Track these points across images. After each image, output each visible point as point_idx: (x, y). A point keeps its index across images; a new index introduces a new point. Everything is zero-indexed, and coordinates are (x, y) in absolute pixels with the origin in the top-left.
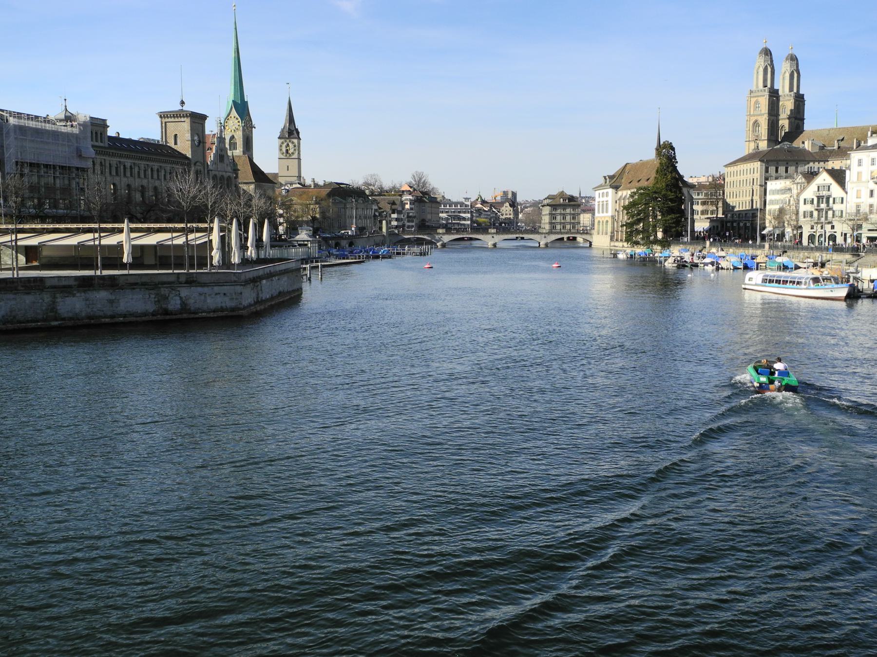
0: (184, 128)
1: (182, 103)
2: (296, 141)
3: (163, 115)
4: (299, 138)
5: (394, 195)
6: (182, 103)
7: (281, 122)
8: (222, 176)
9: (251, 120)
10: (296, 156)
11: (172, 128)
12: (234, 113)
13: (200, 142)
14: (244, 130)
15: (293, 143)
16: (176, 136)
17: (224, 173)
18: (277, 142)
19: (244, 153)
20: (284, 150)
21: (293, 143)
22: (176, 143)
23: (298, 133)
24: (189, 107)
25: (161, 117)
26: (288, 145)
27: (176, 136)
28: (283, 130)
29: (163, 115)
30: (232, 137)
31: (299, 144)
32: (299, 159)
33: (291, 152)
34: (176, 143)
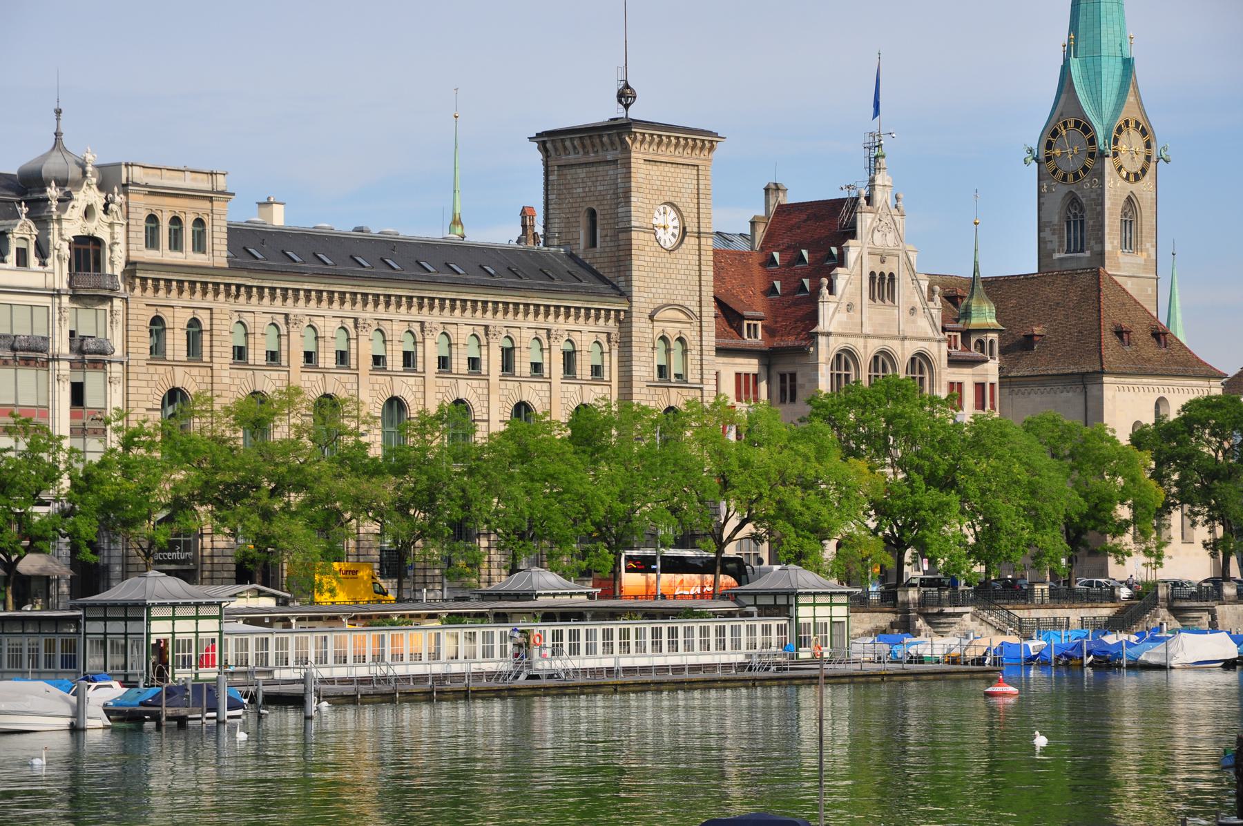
1: (625, 96)
3: (549, 141)
6: (625, 96)
16: (592, 213)
17: (894, 346)
24: (635, 113)
25: (543, 148)
29: (549, 141)
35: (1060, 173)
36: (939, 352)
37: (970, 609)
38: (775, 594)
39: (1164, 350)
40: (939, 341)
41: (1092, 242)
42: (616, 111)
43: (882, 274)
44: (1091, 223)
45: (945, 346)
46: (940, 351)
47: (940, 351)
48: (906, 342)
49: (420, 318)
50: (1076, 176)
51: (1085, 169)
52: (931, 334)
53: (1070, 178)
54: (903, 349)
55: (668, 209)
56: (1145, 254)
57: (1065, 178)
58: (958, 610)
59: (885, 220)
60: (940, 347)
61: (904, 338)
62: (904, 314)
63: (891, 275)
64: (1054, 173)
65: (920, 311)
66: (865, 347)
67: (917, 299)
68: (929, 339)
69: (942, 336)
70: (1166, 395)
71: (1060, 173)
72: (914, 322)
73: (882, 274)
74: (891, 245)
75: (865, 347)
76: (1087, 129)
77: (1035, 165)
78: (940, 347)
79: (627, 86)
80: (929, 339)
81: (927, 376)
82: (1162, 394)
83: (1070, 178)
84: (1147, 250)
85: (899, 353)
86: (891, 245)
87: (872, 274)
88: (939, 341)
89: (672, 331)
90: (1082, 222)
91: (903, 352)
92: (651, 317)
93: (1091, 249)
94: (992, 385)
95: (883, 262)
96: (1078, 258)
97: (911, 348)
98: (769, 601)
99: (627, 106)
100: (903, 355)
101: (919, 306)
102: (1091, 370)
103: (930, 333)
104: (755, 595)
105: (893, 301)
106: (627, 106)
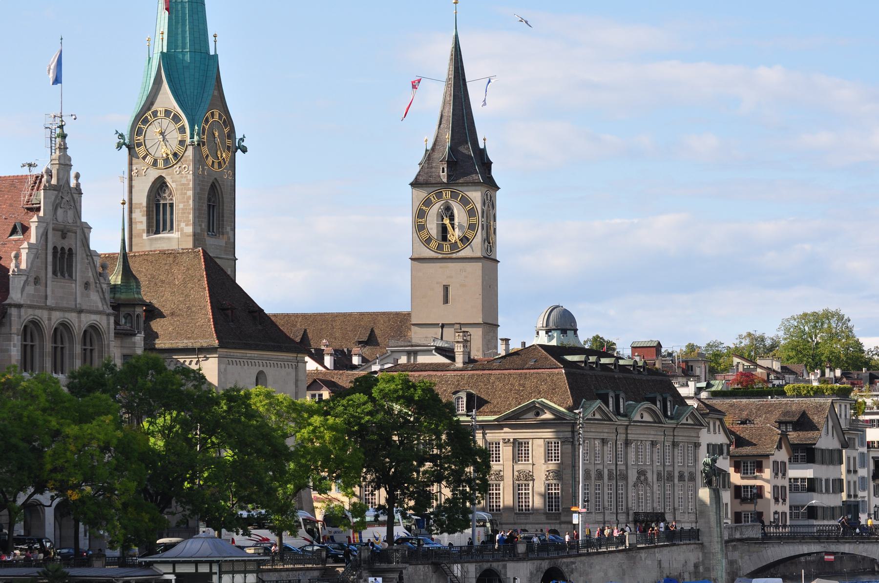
2: (476, 196)
4: (491, 185)
5: (818, 392)
7: (424, 127)
8: (65, 326)
9: (228, 122)
10: (476, 248)
12: (167, 99)
14: (199, 160)
15: (465, 201)
17: (72, 317)
18: (406, 199)
19: (197, 239)
20: (433, 229)
21: (465, 201)
23: (486, 165)
26: (448, 211)
28: (429, 156)
30: (160, 185)
31: (490, 204)
32: (489, 259)
33: (455, 235)
36: (106, 323)
39: (260, 327)
40: (108, 315)
41: (183, 225)
43: (63, 249)
44: (181, 206)
45: (112, 320)
46: (109, 324)
47: (109, 324)
48: (83, 315)
50: (166, 160)
52: (101, 308)
53: (161, 163)
54: (80, 322)
56: (225, 236)
57: (155, 163)
59: (66, 198)
60: (108, 320)
61: (80, 311)
62: (78, 288)
63: (70, 250)
65: (92, 286)
67: (90, 274)
69: (110, 311)
70: (265, 369)
72: (88, 296)
73: (63, 249)
74: (70, 221)
77: (125, 149)
78: (108, 320)
81: (96, 347)
82: (261, 368)
83: (161, 163)
84: (227, 233)
85: (76, 325)
86: (70, 221)
87: (55, 248)
88: (108, 315)
90: (171, 205)
91: (80, 323)
93: (182, 230)
95: (64, 236)
96: (169, 238)
97: (87, 319)
100: (79, 326)
101: (92, 280)
102: (205, 345)
103: (100, 306)
105: (71, 276)
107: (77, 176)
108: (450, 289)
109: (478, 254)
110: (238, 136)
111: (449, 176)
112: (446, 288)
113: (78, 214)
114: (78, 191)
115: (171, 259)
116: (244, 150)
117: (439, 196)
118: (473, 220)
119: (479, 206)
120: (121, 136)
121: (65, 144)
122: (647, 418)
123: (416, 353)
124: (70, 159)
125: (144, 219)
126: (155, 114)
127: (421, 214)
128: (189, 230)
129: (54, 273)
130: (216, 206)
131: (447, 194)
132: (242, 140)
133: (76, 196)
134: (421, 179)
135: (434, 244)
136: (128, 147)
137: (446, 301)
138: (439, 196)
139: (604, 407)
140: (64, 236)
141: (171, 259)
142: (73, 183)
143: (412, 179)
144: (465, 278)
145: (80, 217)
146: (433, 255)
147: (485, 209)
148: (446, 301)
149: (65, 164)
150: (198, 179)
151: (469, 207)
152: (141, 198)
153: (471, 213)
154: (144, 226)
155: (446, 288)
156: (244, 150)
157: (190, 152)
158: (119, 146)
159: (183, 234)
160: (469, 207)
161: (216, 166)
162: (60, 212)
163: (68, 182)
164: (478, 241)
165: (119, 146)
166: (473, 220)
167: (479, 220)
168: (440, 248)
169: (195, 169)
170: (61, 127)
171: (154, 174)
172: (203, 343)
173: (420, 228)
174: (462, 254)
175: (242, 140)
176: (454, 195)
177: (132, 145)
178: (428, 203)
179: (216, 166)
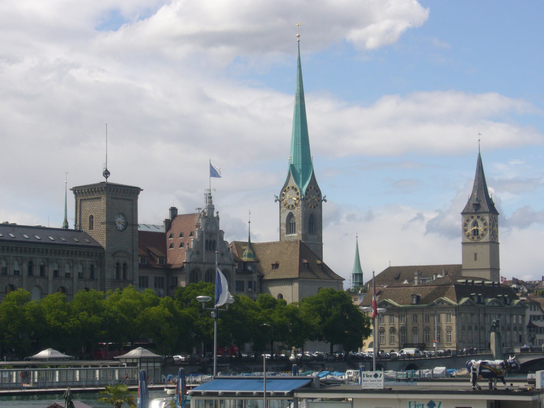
0: (98, 207)
1: (107, 173)
3: (78, 191)
6: (107, 173)
10: (487, 238)
11: (87, 206)
13: (126, 225)
14: (305, 205)
16: (91, 217)
19: (304, 235)
21: (482, 220)
22: (91, 227)
25: (75, 193)
27: (91, 217)
30: (291, 216)
34: (91, 227)
35: (287, 205)
37: (228, 365)
38: (133, 359)
42: (103, 179)
43: (210, 240)
49: (46, 257)
50: (293, 206)
51: (296, 204)
53: (291, 207)
55: (121, 216)
58: (223, 365)
64: (285, 205)
66: (204, 268)
68: (228, 265)
71: (287, 205)
73: (210, 240)
75: (204, 268)
76: (296, 190)
77: (278, 202)
79: (106, 170)
80: (228, 265)
83: (291, 207)
87: (207, 241)
89: (121, 261)
92: (113, 255)
94: (255, 282)
95: (211, 236)
98: (131, 361)
99: (107, 178)
104: (126, 359)
106: (107, 178)
107: (218, 213)
108: (477, 255)
109: (488, 241)
110: (323, 195)
111: (476, 210)
112: (476, 254)
113: (218, 227)
114: (218, 218)
115: (287, 245)
116: (326, 201)
117: (472, 217)
118: (486, 227)
119: (488, 221)
120: (277, 197)
121: (211, 200)
122: (495, 304)
123: (425, 280)
124: (213, 206)
125: (285, 229)
126: (289, 188)
127: (465, 225)
128: (300, 232)
129: (206, 249)
130: (313, 223)
131: (475, 217)
132: (325, 197)
133: (216, 220)
134: (465, 211)
135: (470, 237)
136: (279, 201)
137: (476, 259)
138: (472, 217)
139: (471, 300)
140: (211, 236)
141: (287, 245)
142: (215, 215)
143: (461, 211)
144: (484, 251)
145: (218, 228)
146: (471, 241)
147: (491, 222)
148: (476, 259)
149: (211, 208)
150: (304, 213)
151: (484, 221)
152: (284, 221)
153: (485, 224)
154: (285, 232)
155: (476, 254)
156: (326, 201)
157: (300, 202)
158: (276, 201)
159: (299, 234)
160: (484, 221)
161: (312, 207)
162: (209, 227)
163: (212, 215)
164: (488, 234)
165: (276, 201)
166: (486, 227)
167: (488, 227)
168: (473, 238)
169: (303, 209)
170: (210, 194)
171: (288, 211)
172: (293, 276)
173: (465, 230)
174: (482, 241)
175: (325, 197)
176: (478, 217)
177: (280, 200)
178: (468, 221)
179: (312, 207)
